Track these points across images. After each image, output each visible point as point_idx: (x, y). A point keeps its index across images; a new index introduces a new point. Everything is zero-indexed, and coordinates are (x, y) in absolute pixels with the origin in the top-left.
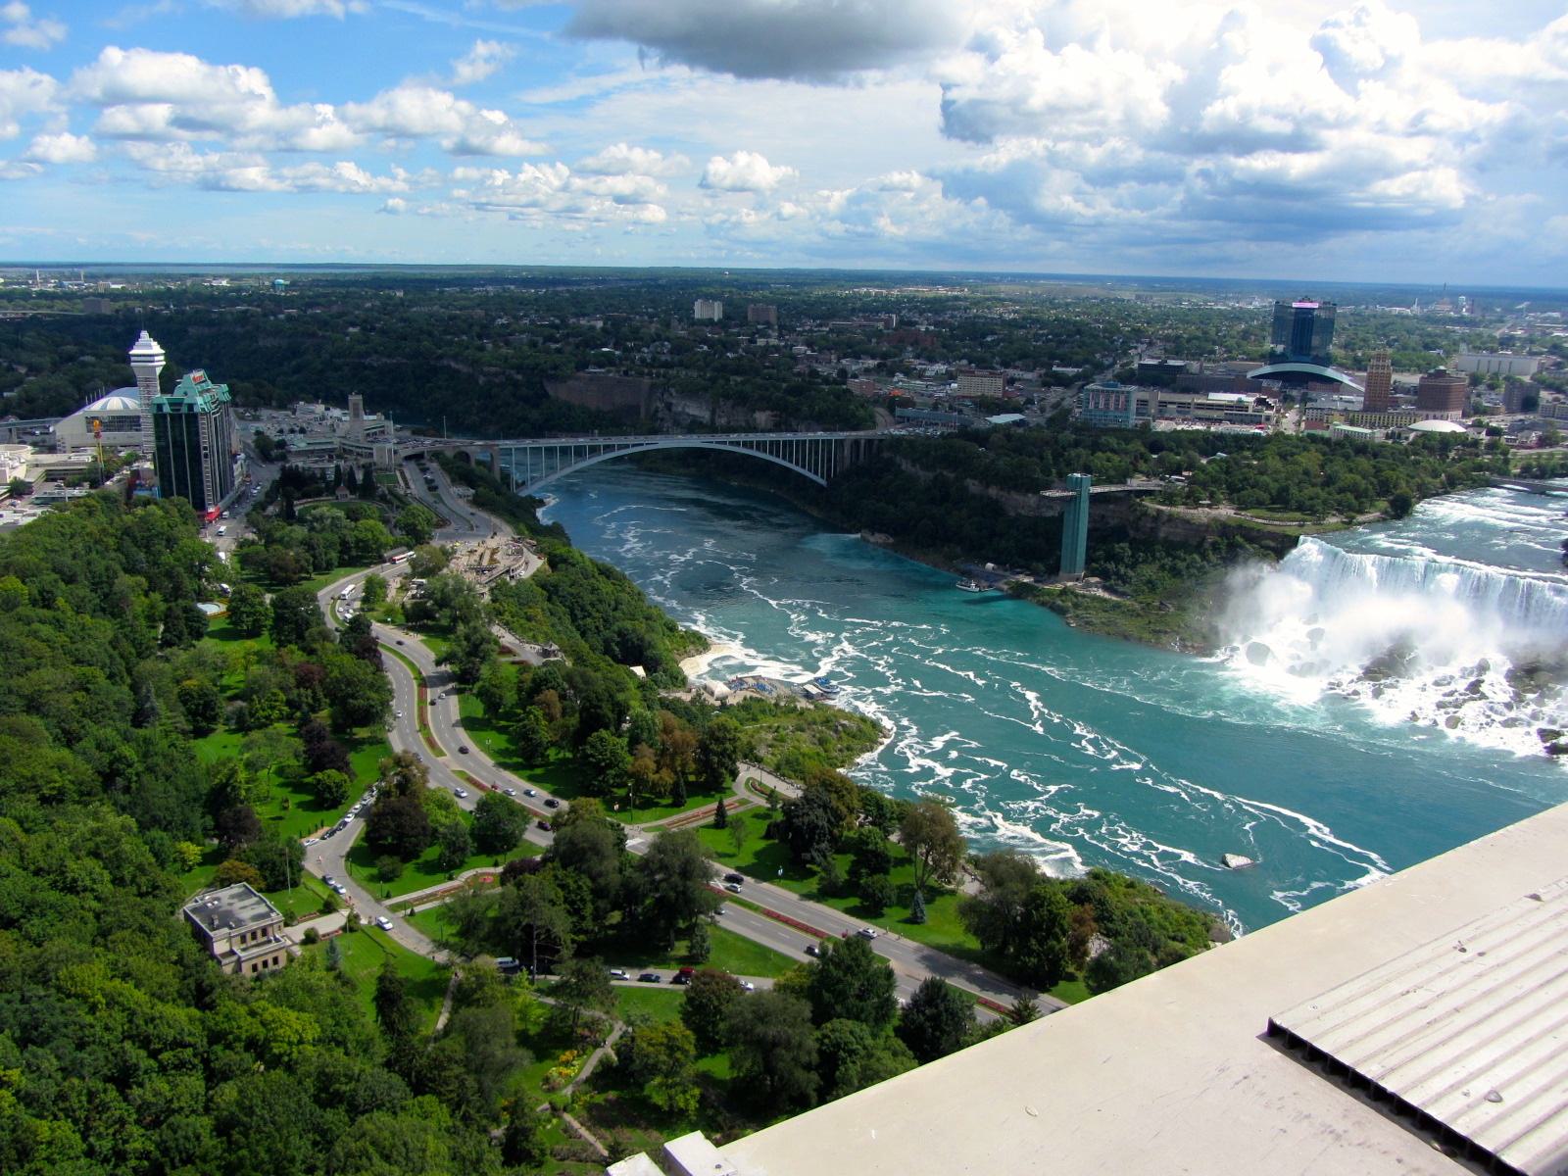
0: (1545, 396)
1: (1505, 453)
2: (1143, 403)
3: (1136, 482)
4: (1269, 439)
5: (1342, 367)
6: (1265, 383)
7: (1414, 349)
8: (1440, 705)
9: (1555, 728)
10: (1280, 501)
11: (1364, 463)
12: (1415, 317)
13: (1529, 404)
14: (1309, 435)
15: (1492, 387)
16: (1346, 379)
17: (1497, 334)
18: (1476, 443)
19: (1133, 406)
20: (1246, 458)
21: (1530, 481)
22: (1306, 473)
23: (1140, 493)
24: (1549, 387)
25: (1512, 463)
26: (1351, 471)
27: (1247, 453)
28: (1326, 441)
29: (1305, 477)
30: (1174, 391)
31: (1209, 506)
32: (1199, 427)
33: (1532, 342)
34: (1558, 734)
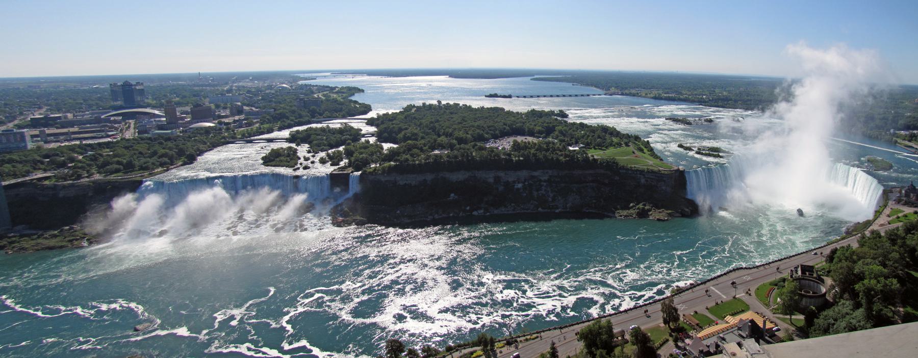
0: (245, 108)
1: (233, 131)
2: (33, 136)
3: (40, 175)
4: (118, 142)
5: (154, 107)
6: (112, 118)
7: (189, 97)
8: (229, 229)
9: (276, 222)
10: (129, 167)
11: (170, 144)
12: (188, 85)
13: (240, 111)
14: (140, 138)
15: (225, 108)
16: (157, 112)
17: (225, 89)
18: (220, 129)
19: (28, 138)
20: (106, 152)
21: (245, 139)
22: (141, 153)
23: (40, 179)
24: (248, 105)
25: (237, 133)
26: (164, 148)
27: (108, 150)
28: (150, 139)
29: (140, 155)
30: (57, 128)
31: (87, 177)
32: (78, 142)
33: (240, 90)
34: (275, 225)
